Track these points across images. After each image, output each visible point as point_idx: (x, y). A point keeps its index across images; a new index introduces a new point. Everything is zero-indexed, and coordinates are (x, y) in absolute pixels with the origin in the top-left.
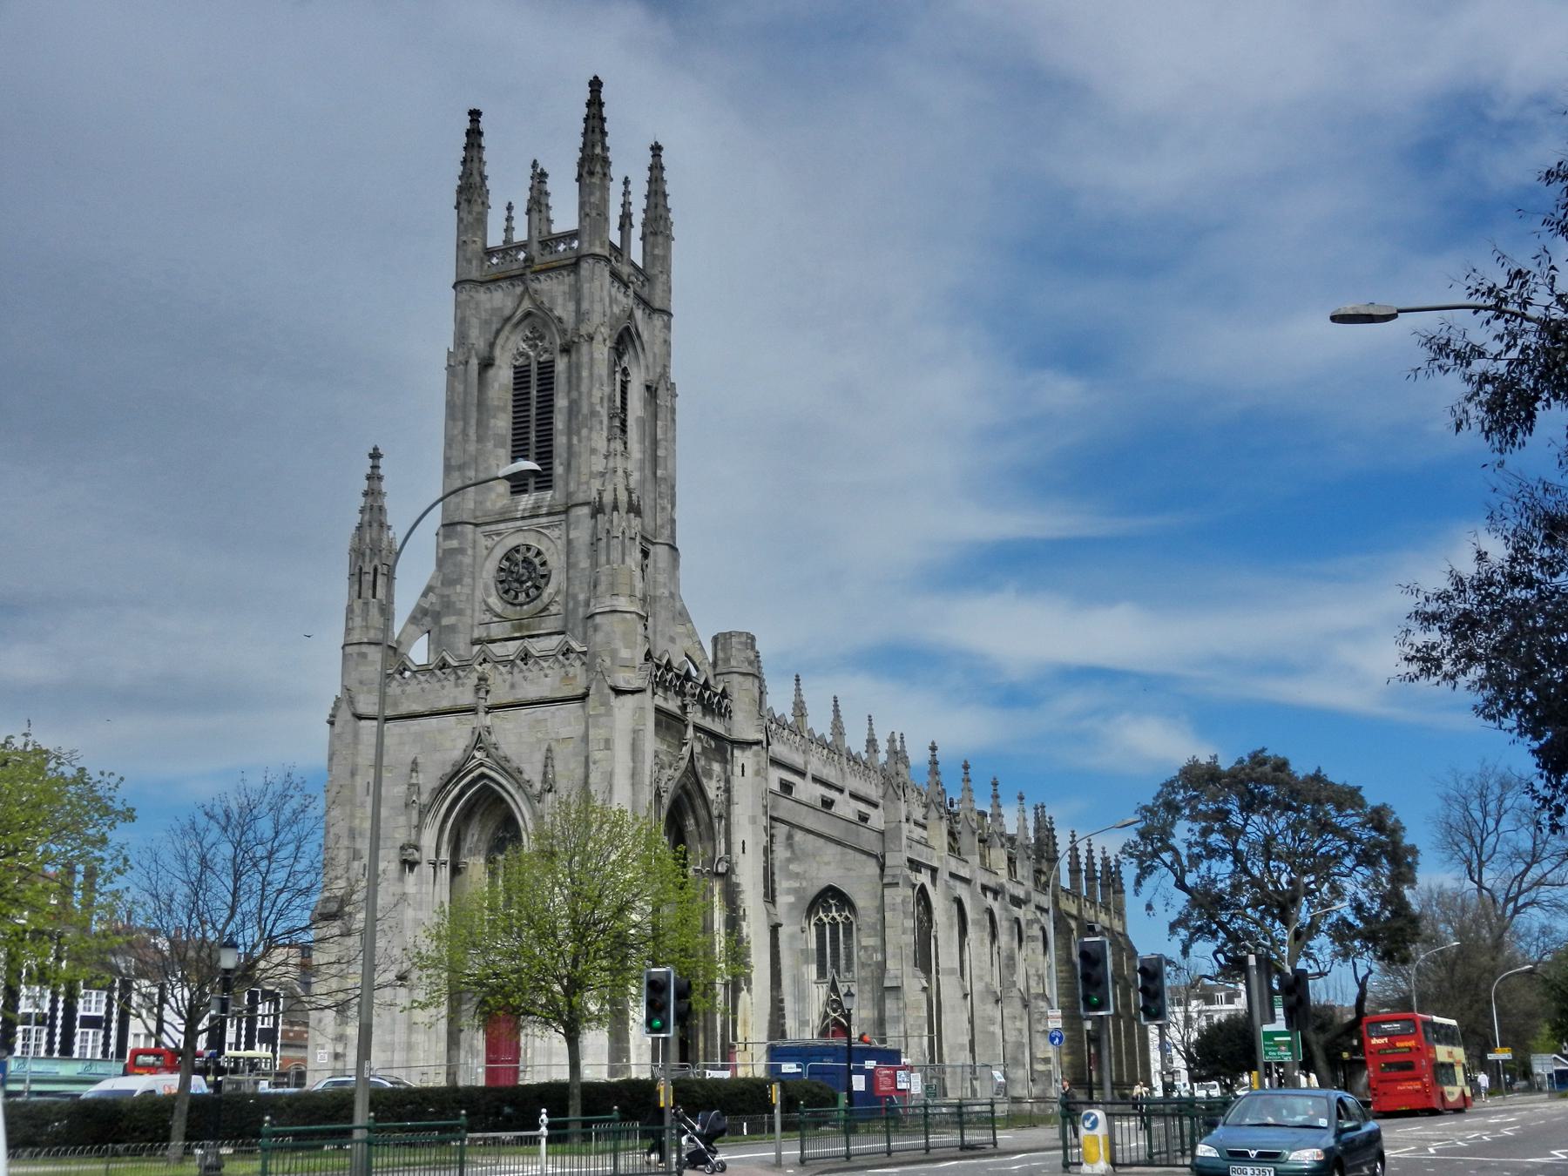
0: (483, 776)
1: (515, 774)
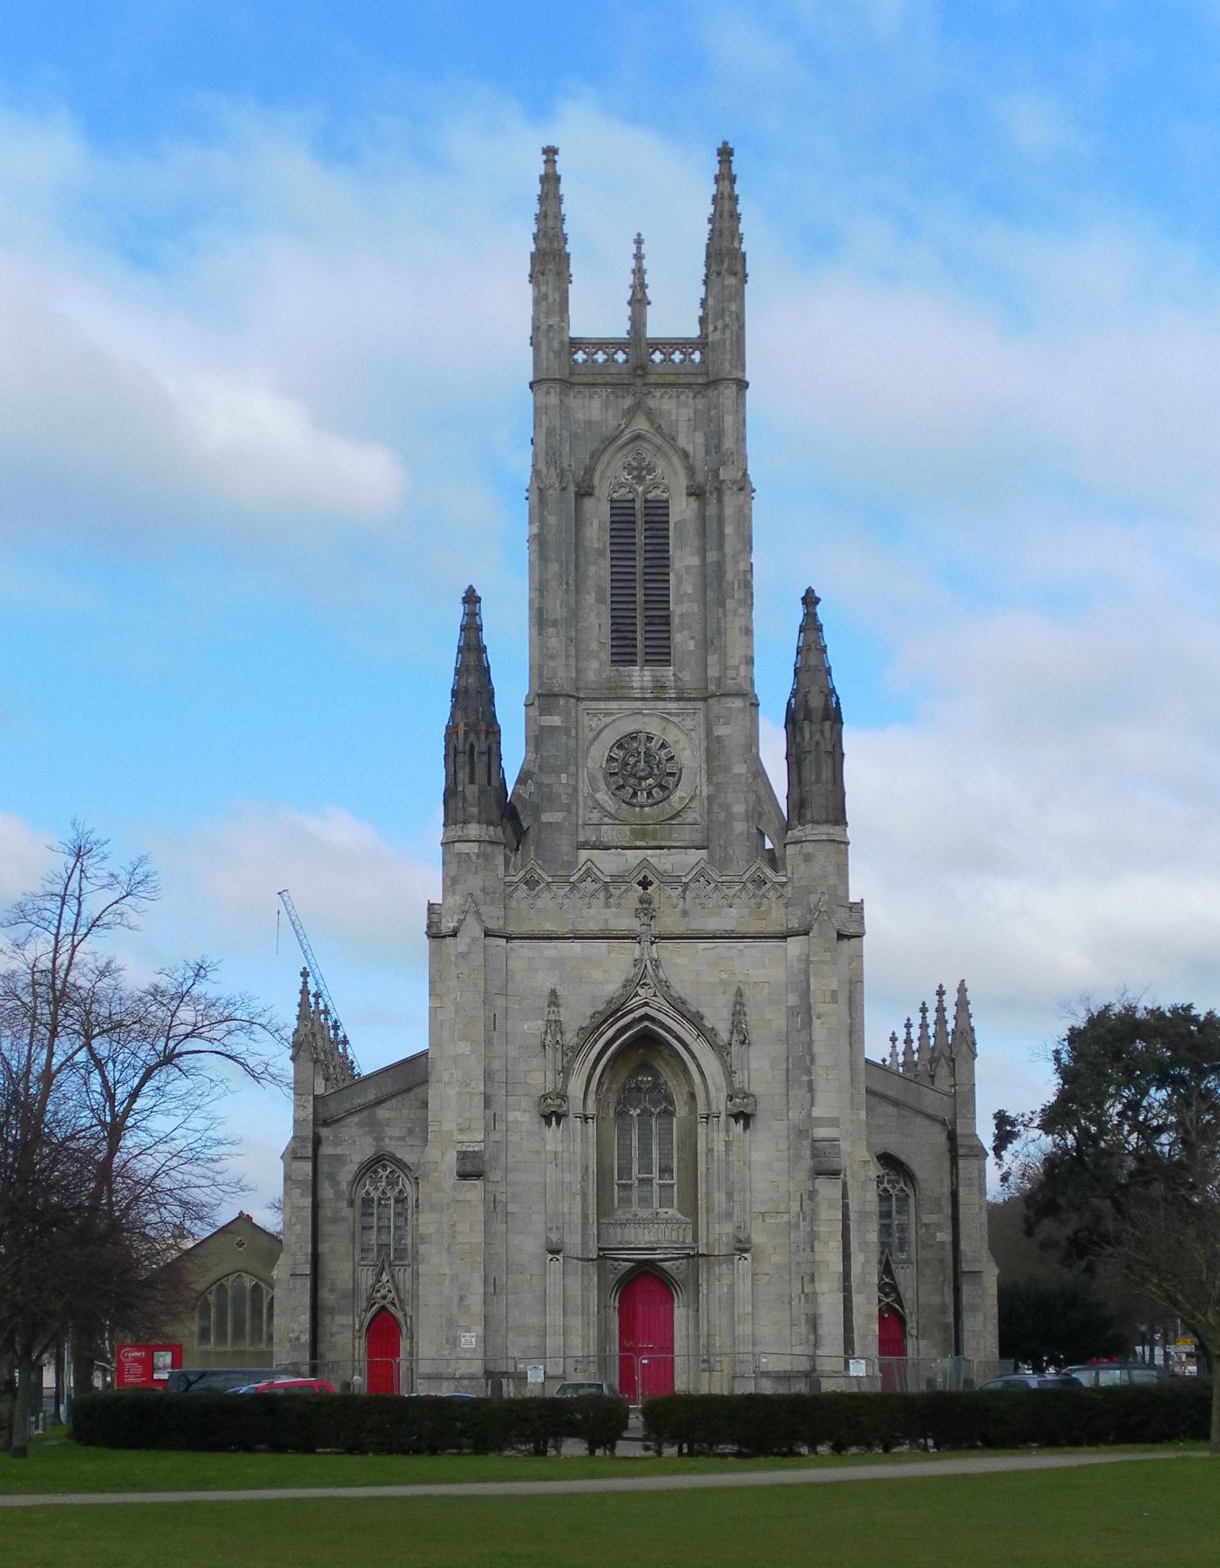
0: (646, 1017)
1: (695, 1020)
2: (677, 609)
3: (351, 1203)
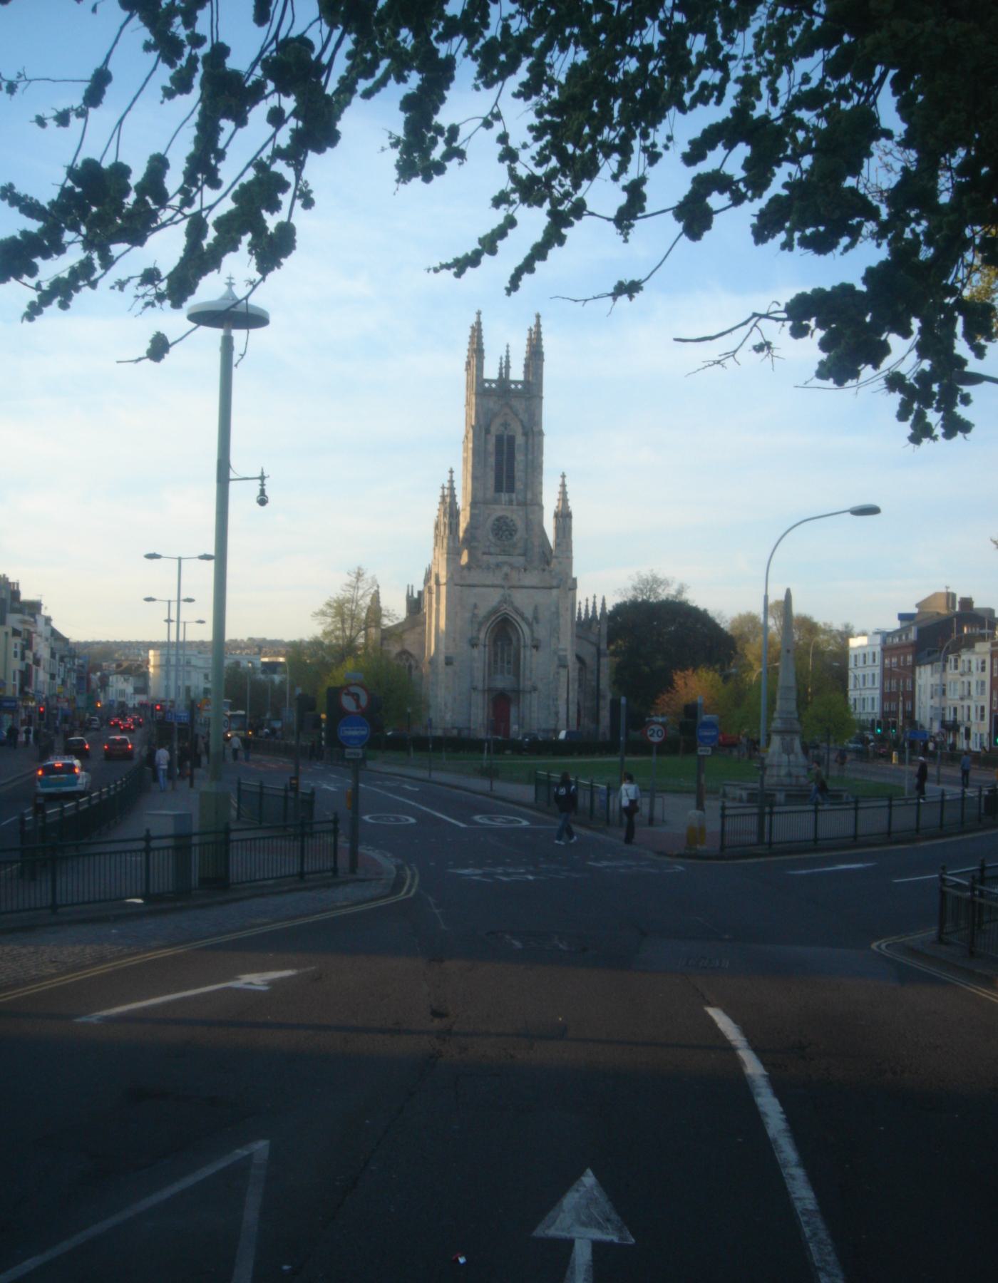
1: (521, 615)
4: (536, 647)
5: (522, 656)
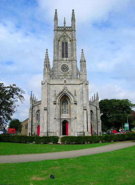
0: (65, 93)
1: (70, 93)
2: (69, 52)
3: (36, 115)
4: (76, 104)
5: (71, 107)
